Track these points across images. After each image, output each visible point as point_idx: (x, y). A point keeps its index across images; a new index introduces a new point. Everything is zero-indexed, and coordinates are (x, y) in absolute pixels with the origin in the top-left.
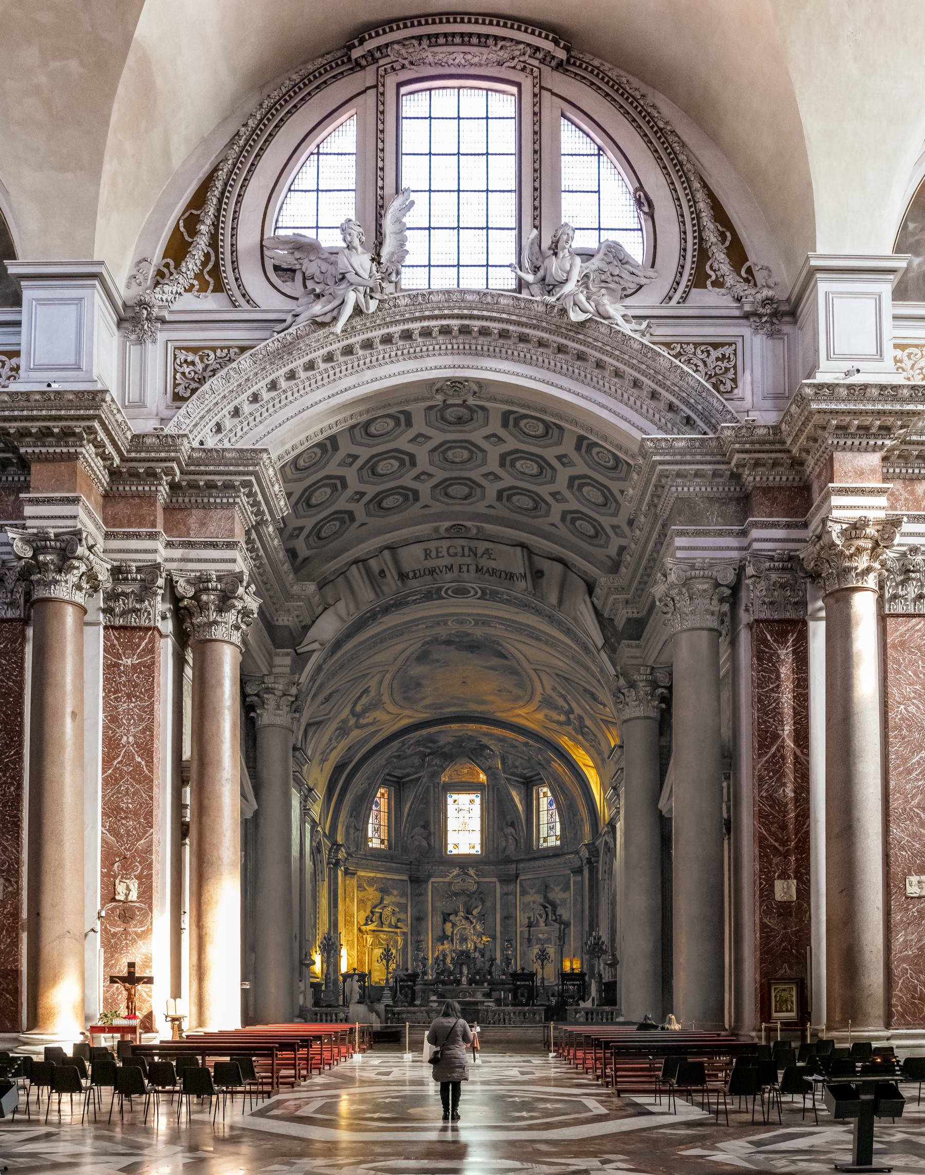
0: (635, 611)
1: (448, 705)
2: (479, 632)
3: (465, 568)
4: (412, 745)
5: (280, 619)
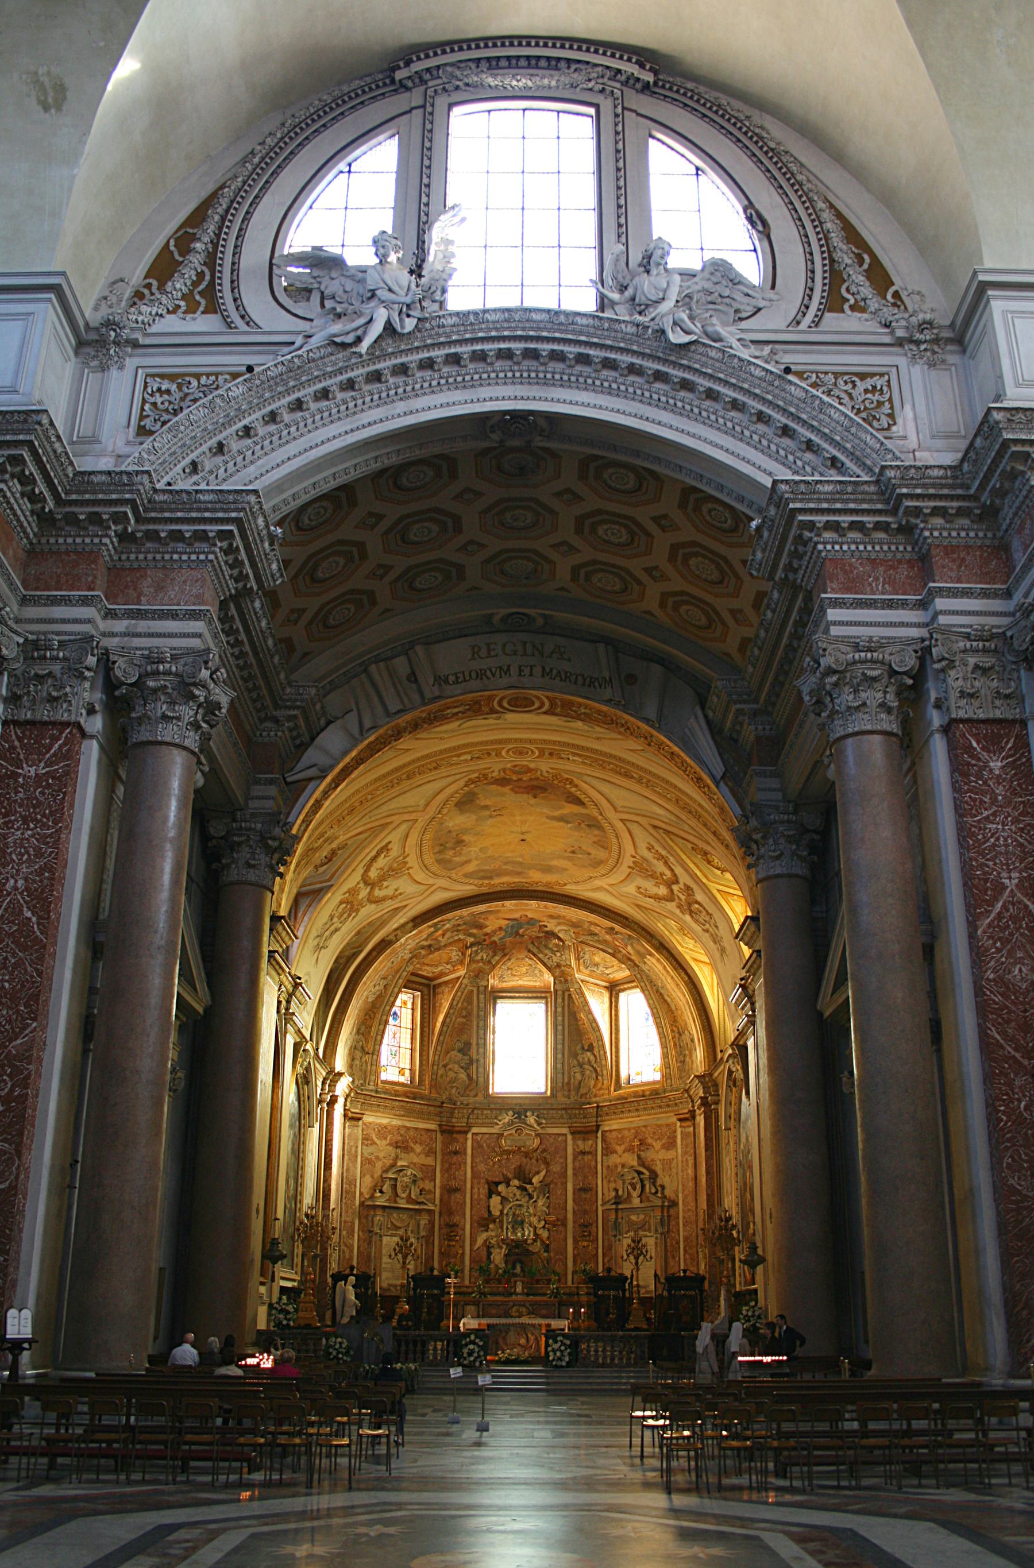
0: (768, 727)
1: (500, 873)
2: (545, 766)
3: (527, 671)
4: (448, 930)
5: (265, 734)
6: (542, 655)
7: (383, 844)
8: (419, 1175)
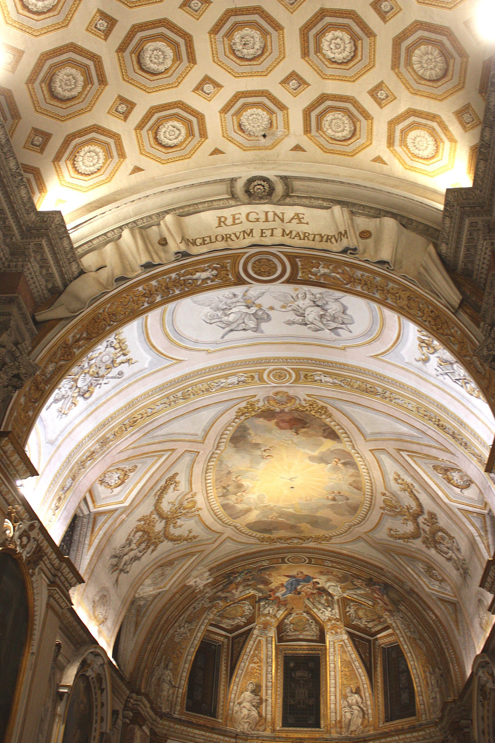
6: (282, 220)
7: (171, 474)
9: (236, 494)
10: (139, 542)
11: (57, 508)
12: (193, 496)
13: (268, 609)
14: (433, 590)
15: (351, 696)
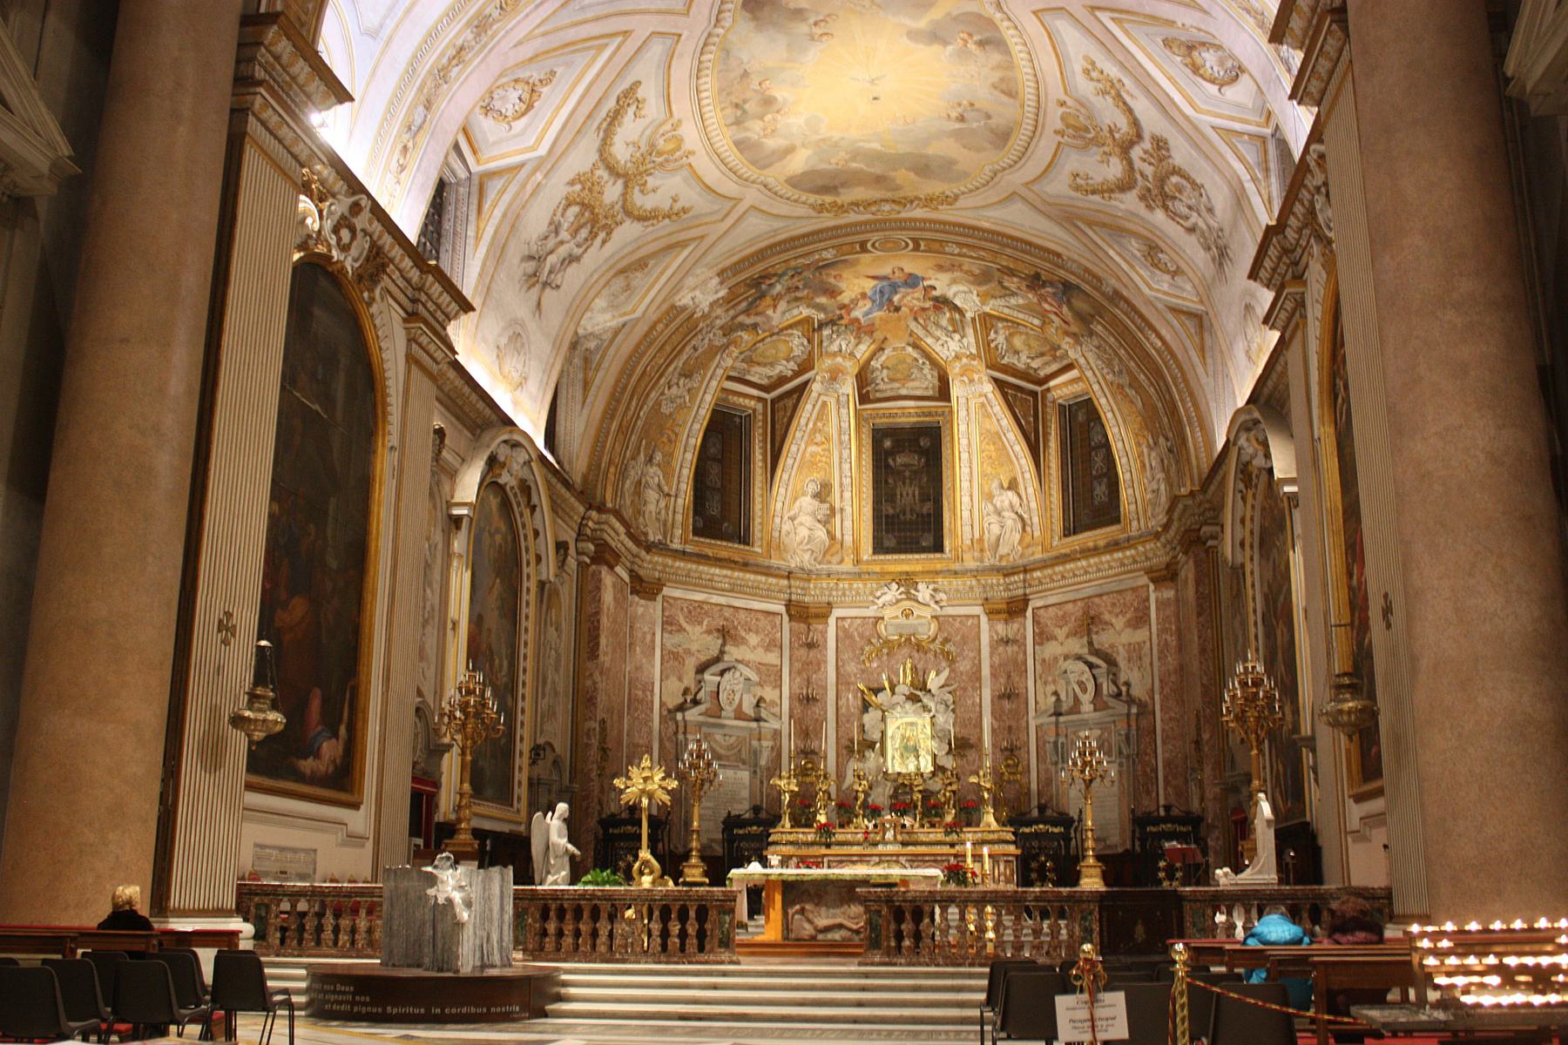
7: (625, 85)
8: (754, 677)
9: (762, 118)
10: (574, 227)
11: (402, 168)
12: (675, 127)
13: (837, 342)
14: (1158, 291)
15: (1001, 494)
